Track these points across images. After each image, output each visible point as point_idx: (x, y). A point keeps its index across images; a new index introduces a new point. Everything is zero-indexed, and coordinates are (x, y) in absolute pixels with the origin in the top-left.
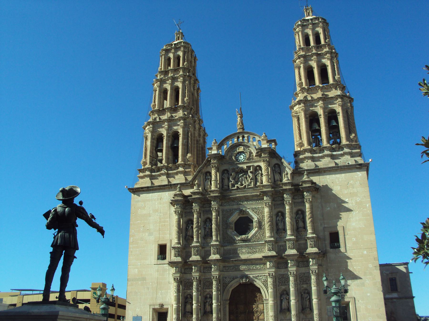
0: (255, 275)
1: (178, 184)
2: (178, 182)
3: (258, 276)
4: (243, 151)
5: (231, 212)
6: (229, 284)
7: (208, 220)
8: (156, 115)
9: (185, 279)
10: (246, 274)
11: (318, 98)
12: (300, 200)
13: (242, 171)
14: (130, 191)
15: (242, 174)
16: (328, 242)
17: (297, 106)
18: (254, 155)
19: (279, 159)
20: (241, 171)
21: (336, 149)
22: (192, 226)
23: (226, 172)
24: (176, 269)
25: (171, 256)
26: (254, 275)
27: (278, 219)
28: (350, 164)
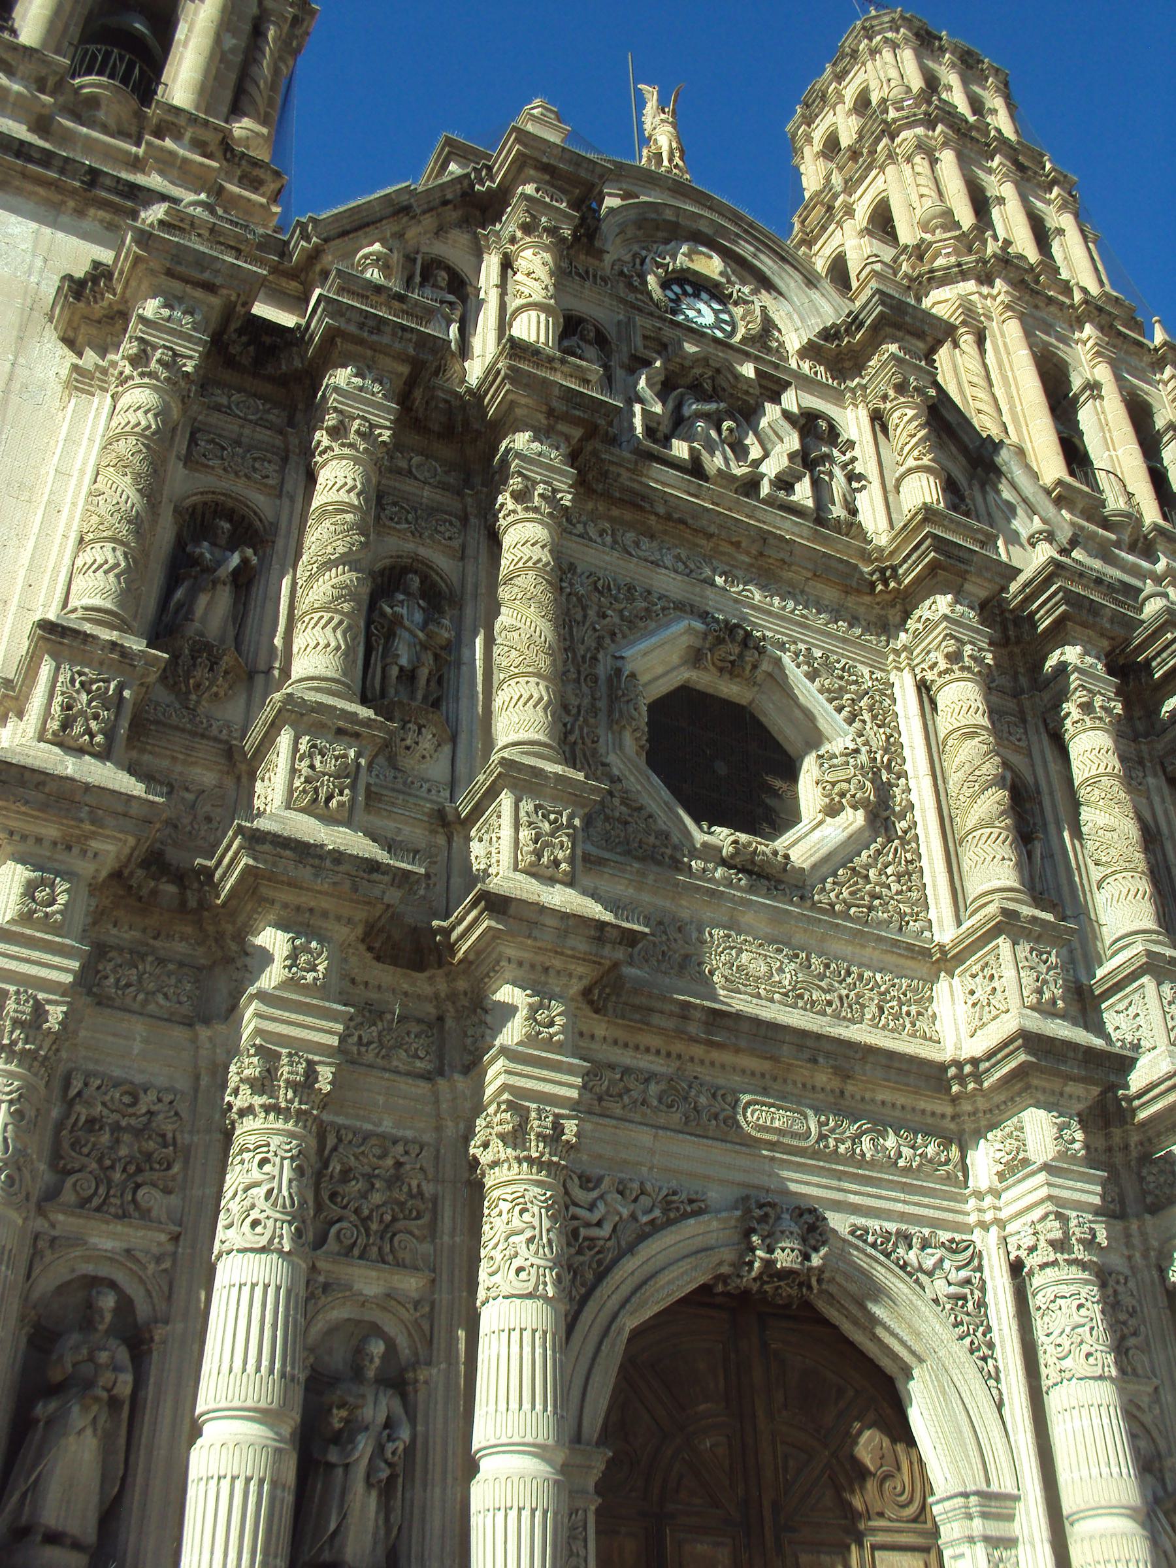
4: (717, 285)
6: (631, 1249)
7: (415, 582)
9: (88, 1075)
10: (793, 1187)
24: (42, 883)
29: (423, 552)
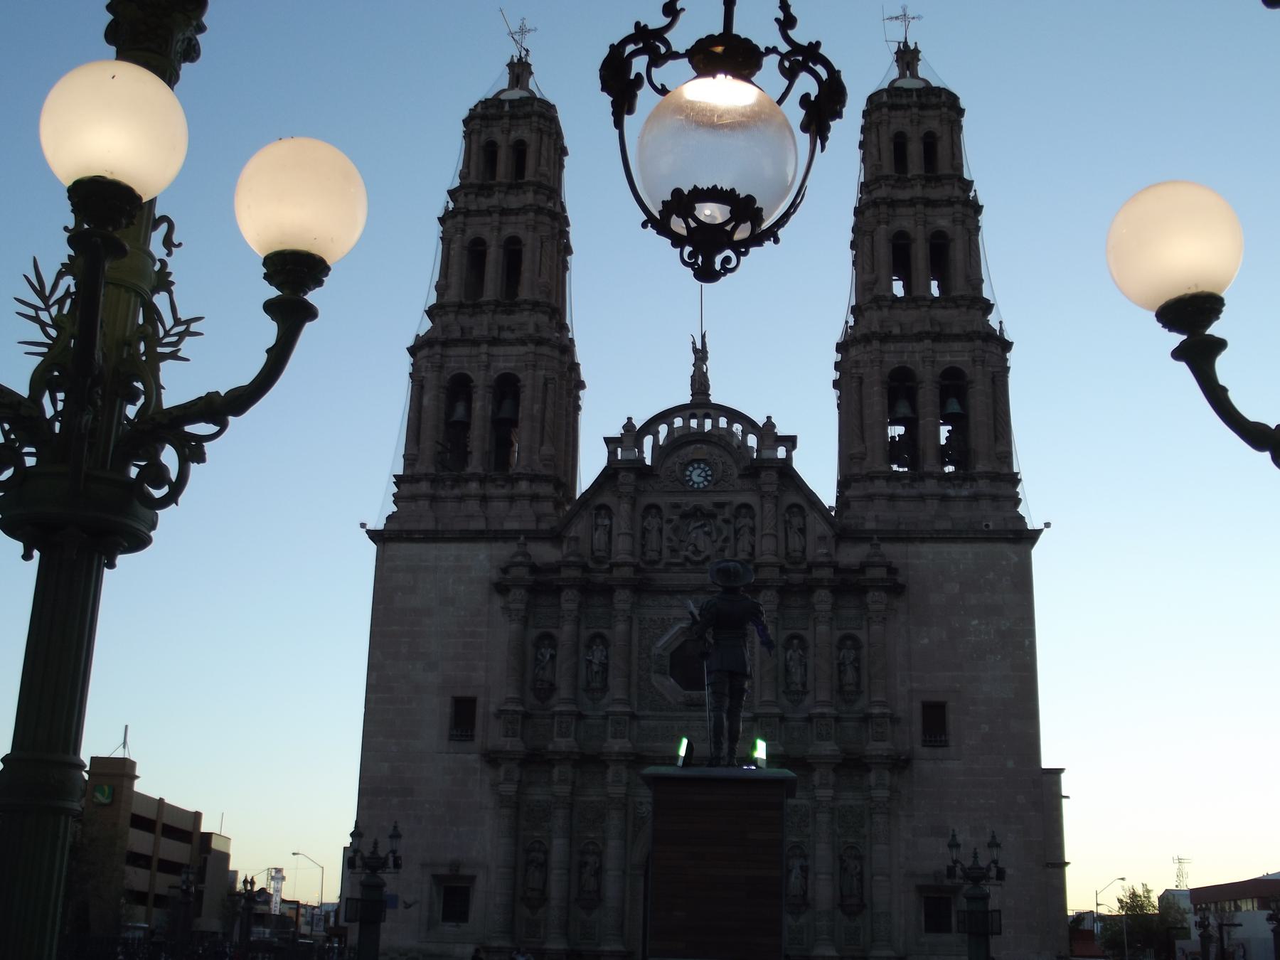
1: (518, 532)
4: (705, 459)
8: (451, 316)
11: (920, 333)
13: (699, 513)
14: (371, 538)
16: (917, 727)
21: (956, 482)
22: (553, 652)
23: (654, 511)
25: (490, 733)
27: (791, 657)
28: (991, 528)
29: (600, 630)
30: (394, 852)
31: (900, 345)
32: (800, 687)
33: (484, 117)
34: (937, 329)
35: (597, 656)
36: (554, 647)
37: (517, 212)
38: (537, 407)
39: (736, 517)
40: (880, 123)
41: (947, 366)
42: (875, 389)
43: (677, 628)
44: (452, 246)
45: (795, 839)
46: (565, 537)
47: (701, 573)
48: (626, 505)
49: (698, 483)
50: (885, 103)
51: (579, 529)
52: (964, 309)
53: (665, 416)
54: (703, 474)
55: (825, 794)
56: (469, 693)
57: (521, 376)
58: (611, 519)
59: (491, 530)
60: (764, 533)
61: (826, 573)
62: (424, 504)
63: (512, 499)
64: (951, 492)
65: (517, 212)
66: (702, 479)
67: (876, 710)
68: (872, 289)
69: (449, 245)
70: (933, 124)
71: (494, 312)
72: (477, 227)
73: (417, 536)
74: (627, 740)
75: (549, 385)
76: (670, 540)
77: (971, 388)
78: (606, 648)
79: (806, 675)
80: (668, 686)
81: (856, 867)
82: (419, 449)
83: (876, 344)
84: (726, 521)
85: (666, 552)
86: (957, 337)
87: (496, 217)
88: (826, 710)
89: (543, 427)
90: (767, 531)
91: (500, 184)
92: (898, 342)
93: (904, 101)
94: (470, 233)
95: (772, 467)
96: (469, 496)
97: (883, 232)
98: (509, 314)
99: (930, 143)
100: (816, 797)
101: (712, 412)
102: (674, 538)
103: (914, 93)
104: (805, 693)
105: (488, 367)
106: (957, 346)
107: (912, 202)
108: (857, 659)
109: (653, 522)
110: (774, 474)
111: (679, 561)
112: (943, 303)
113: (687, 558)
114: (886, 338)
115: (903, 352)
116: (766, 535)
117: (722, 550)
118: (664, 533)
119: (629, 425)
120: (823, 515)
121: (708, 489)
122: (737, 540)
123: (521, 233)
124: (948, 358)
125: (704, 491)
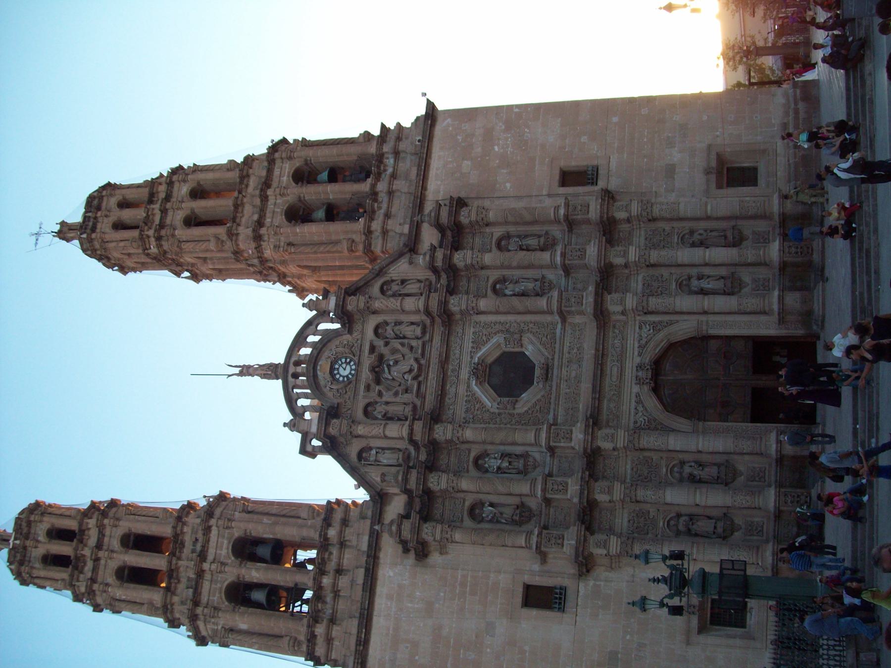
0: (633, 401)
2: (366, 538)
3: (639, 343)
4: (331, 363)
5: (472, 399)
8: (176, 599)
11: (261, 196)
12: (477, 240)
13: (377, 369)
15: (386, 369)
17: (264, 244)
18: (348, 336)
19: (373, 279)
20: (376, 372)
23: (369, 409)
26: (636, 353)
29: (471, 459)
30: (665, 558)
31: (269, 214)
32: (538, 283)
33: (21, 563)
34: (260, 187)
35: (494, 463)
36: (482, 504)
37: (101, 535)
38: (265, 520)
39: (387, 338)
40: (103, 241)
41: (291, 179)
42: (298, 230)
43: (476, 389)
44: (118, 598)
45: (674, 287)
46: (381, 490)
47: (429, 367)
48: (359, 428)
49: (351, 370)
50: (88, 235)
51: (375, 475)
52: (251, 171)
53: (291, 401)
54: (344, 365)
55: (633, 254)
56: (520, 590)
57: (236, 535)
58: (371, 449)
59: (366, 561)
60: (399, 308)
61: (439, 254)
62: (336, 631)
63: (342, 544)
64: (390, 170)
65: (101, 535)
66: (348, 368)
67: (562, 211)
68: (223, 241)
69: (117, 600)
70: (113, 201)
71: (179, 559)
72: (107, 574)
73: (363, 636)
74: (574, 428)
75: (249, 509)
76: (396, 394)
77: (311, 160)
78: (488, 455)
79: (528, 279)
80: (528, 399)
81: (700, 234)
82: (287, 636)
83: (263, 231)
84: (387, 344)
85: (407, 397)
86: (270, 171)
87: (101, 554)
88: (559, 253)
89: (284, 516)
90: (398, 304)
91: (76, 549)
92: (265, 216)
93: (91, 224)
94: (111, 579)
95: (344, 298)
96: (334, 585)
97: (182, 233)
98: (184, 546)
99: (124, 204)
100: (635, 261)
101: (293, 359)
102: (395, 390)
103: (88, 214)
104: (543, 277)
105: (223, 564)
106: (277, 172)
107: (164, 211)
108: (519, 236)
109: (380, 409)
110: (350, 298)
111: (415, 387)
112: (243, 186)
113: (415, 378)
114: (260, 223)
115: (274, 212)
116: (401, 306)
117: (411, 348)
118: (389, 400)
119: (292, 426)
120: (392, 262)
121: (357, 361)
122: (404, 337)
123: (119, 532)
124: (285, 179)
125: (358, 364)
